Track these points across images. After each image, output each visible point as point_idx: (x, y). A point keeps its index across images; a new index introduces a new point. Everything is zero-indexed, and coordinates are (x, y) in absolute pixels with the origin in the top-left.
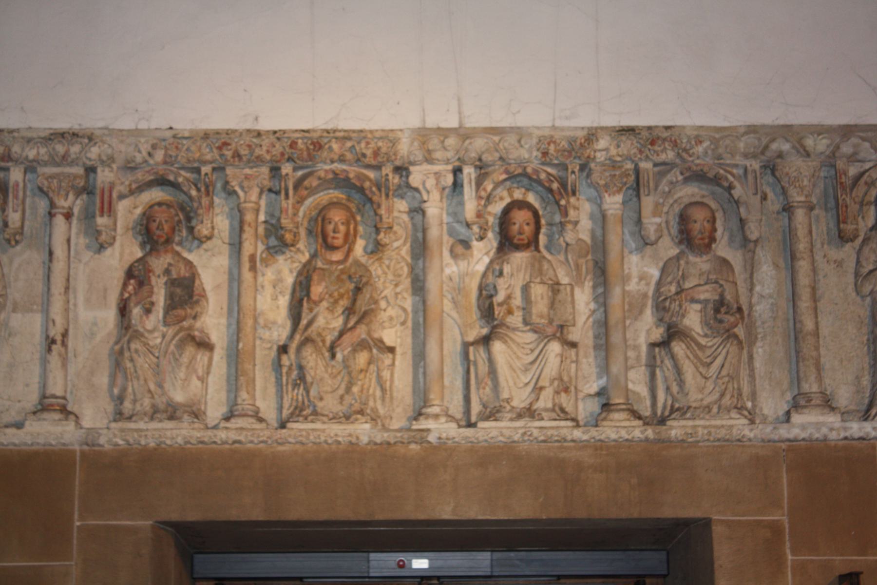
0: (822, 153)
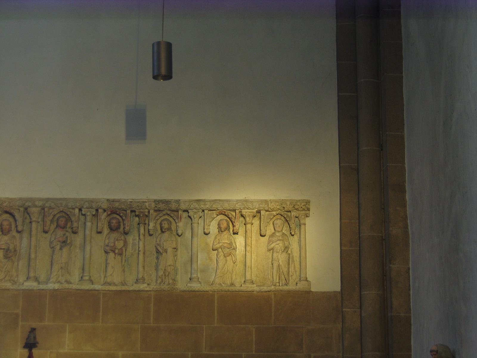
0: (41, 206)
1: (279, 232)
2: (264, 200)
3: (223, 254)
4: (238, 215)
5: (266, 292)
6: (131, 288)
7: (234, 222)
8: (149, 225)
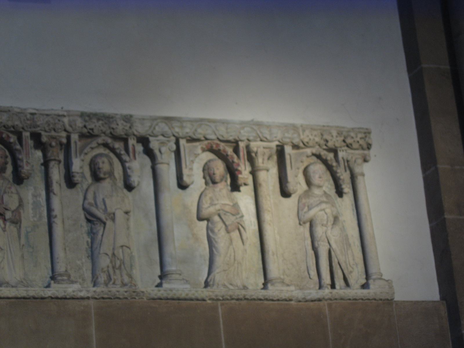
3: (224, 226)
5: (315, 301)
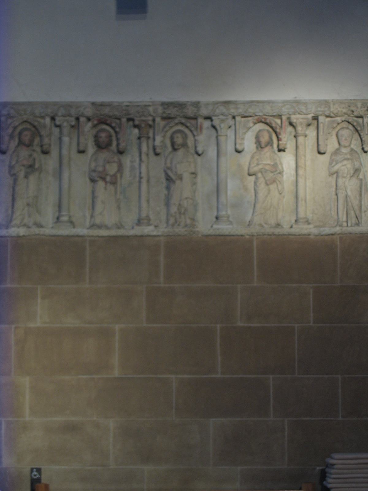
1: (345, 147)
2: (323, 100)
4: (286, 123)
6: (131, 233)
7: (280, 134)
8: (154, 140)
